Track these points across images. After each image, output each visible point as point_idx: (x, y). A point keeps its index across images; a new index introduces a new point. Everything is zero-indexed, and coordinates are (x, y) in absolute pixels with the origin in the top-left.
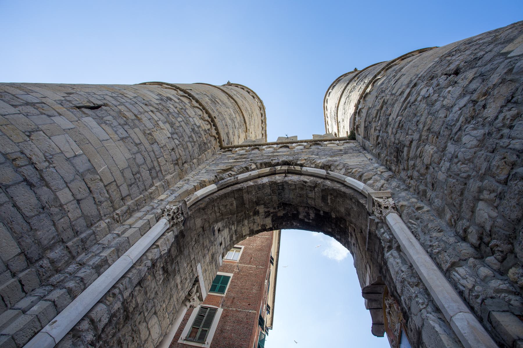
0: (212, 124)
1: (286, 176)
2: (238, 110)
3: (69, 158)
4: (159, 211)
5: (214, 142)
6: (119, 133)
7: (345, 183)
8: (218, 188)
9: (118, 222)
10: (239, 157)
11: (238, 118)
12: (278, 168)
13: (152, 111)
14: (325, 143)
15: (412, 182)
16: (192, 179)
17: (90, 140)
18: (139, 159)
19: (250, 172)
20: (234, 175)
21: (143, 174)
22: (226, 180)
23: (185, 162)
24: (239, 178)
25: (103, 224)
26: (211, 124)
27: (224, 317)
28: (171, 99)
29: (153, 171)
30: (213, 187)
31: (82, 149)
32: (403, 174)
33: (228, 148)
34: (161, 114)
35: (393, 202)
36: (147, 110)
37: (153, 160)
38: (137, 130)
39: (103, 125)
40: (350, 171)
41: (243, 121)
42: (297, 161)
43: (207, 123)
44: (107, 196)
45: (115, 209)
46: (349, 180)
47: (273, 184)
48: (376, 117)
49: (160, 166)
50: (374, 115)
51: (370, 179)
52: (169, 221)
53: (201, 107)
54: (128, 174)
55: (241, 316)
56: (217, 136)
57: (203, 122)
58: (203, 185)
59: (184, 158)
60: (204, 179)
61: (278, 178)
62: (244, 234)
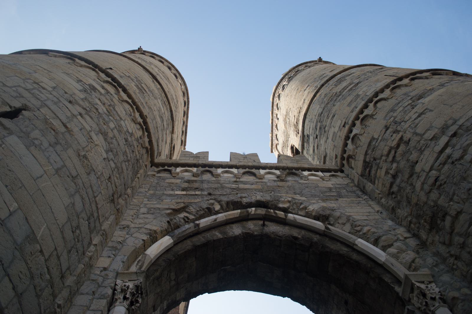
0: (144, 127)
1: (264, 225)
3: (3, 221)
4: (110, 292)
5: (145, 156)
6: (52, 161)
7: (355, 247)
8: (174, 242)
10: (186, 185)
11: (166, 113)
13: (81, 114)
14: (306, 173)
15: (459, 264)
16: (133, 225)
19: (214, 217)
20: (193, 221)
21: (82, 229)
22: (183, 229)
24: (201, 226)
28: (94, 89)
29: (92, 220)
30: (166, 241)
32: (442, 249)
33: (163, 165)
35: (437, 290)
36: (76, 113)
38: (70, 151)
39: (32, 148)
40: (358, 228)
41: (170, 117)
42: (277, 203)
43: (139, 127)
45: (54, 296)
46: (362, 243)
47: (247, 237)
48: (388, 155)
50: (385, 153)
51: (390, 246)
53: (130, 101)
56: (149, 147)
58: (154, 238)
60: (155, 228)
61: (252, 226)
62: (178, 299)
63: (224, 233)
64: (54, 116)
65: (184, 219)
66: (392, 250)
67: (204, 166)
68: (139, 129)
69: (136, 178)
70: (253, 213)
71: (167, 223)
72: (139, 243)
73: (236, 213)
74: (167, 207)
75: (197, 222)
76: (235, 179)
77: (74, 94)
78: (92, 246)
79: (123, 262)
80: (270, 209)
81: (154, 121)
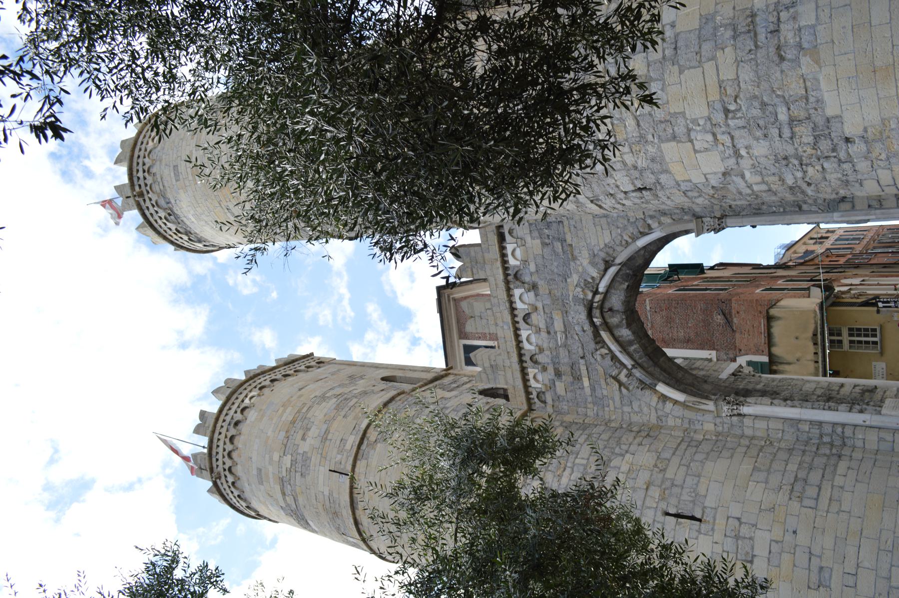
1: (611, 310)
4: (735, 419)
6: (695, 482)
12: (597, 321)
18: (699, 457)
19: (618, 354)
25: (783, 445)
30: (661, 388)
31: (748, 484)
33: (529, 400)
35: (709, 219)
40: (624, 243)
45: (763, 447)
49: (679, 444)
51: (649, 225)
54: (726, 453)
55: (658, 319)
58: (664, 398)
59: (633, 434)
63: (631, 343)
64: (648, 499)
66: (654, 225)
67: (521, 361)
72: (676, 407)
73: (604, 335)
74: (617, 393)
75: (630, 367)
76: (544, 334)
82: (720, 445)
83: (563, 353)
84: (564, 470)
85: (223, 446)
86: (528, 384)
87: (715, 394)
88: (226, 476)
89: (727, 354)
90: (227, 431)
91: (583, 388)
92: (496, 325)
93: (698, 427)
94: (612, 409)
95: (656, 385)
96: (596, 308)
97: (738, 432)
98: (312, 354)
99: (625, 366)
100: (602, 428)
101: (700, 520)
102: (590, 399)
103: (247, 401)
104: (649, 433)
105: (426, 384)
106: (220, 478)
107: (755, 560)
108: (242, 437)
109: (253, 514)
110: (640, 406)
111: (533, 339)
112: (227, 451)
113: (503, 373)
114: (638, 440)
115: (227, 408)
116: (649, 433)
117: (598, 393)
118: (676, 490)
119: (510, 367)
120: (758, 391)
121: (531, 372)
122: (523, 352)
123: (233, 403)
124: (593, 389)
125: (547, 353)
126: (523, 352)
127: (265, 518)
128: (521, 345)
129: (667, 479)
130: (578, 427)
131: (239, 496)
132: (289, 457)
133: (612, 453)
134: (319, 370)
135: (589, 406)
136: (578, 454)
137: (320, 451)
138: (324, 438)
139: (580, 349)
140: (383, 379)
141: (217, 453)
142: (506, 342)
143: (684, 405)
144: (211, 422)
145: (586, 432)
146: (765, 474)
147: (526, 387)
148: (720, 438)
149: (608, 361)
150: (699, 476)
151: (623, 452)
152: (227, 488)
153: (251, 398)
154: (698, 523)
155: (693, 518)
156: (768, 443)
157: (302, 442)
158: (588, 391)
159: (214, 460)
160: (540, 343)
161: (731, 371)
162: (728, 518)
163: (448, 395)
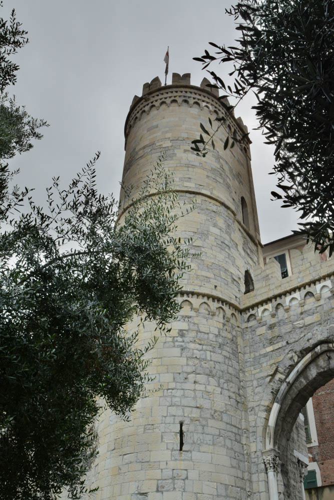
2: (214, 206)
4: (263, 466)
9: (251, 494)
13: (195, 382)
17: (210, 470)
18: (228, 443)
21: (237, 450)
23: (239, 390)
24: (291, 382)
26: (221, 307)
27: (317, 407)
30: (276, 407)
31: (214, 482)
33: (247, 309)
34: (199, 374)
37: (231, 430)
44: (239, 489)
49: (235, 427)
52: (274, 471)
54: (234, 462)
57: (216, 318)
58: (269, 410)
63: (306, 378)
65: (279, 380)
67: (275, 297)
68: (219, 313)
69: (239, 354)
70: (319, 351)
71: (271, 394)
73: (308, 356)
74: (266, 374)
75: (287, 380)
76: (299, 310)
77: (182, 366)
78: (245, 446)
79: (261, 442)
80: (330, 343)
81: (221, 272)
82: (241, 457)
83: (288, 327)
84: (200, 344)
85: (168, 96)
86: (260, 306)
87: (279, 448)
88: (148, 105)
89: (317, 454)
90: (180, 96)
91: (264, 348)
92: (300, 272)
93: (252, 439)
94: (253, 372)
95: (277, 402)
96: (328, 347)
97: (254, 470)
98: (251, 142)
99: (287, 376)
100: (237, 367)
101: (181, 449)
102: (257, 354)
103: (204, 104)
104: (240, 402)
105: (245, 230)
106: (146, 101)
107: (159, 494)
108: (177, 108)
109: (127, 132)
110: (260, 393)
111: (294, 303)
112: (165, 100)
113: (264, 285)
114: (233, 395)
115: (196, 91)
116: (240, 402)
117: (263, 360)
118: (200, 428)
119: (270, 290)
120: (288, 481)
121: (269, 306)
122: (283, 297)
123: (200, 95)
124: (265, 355)
125: (286, 315)
126: (283, 297)
127: (126, 141)
128: (288, 294)
129: (207, 421)
130: (235, 349)
131: (136, 118)
132: (170, 144)
133: (219, 378)
134: (239, 149)
135: (252, 355)
136: (214, 352)
137: (178, 165)
138: (189, 166)
139: (294, 340)
140: (243, 199)
141: (162, 94)
142: (288, 282)
143: (266, 426)
144: (183, 83)
145: (231, 355)
146: (224, 494)
147: (257, 305)
148: (246, 457)
149: (288, 363)
150: (214, 444)
151: (221, 386)
152: (140, 108)
153: (207, 106)
154: (179, 449)
155: (182, 444)
156: (249, 493)
157: (182, 150)
158: (263, 351)
159: (158, 93)
160: (292, 308)
161: (301, 459)
162: (186, 470)
163: (240, 248)
